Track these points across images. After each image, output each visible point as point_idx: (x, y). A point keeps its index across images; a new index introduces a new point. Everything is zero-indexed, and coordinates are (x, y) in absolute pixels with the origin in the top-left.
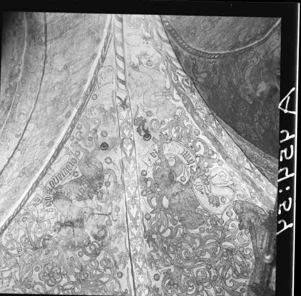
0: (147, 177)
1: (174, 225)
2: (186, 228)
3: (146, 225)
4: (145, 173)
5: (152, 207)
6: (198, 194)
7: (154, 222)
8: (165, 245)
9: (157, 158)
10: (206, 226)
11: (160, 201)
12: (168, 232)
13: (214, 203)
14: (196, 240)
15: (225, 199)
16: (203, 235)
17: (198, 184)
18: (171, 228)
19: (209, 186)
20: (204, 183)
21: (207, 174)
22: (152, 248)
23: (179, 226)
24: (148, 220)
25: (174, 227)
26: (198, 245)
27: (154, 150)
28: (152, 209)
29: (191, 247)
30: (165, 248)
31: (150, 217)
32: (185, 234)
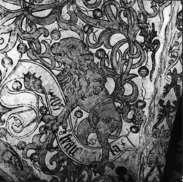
0: (132, 124)
1: (102, 50)
2: (82, 42)
3: (150, 60)
4: (134, 130)
5: (133, 84)
6: (57, 92)
7: (135, 61)
8: (125, 20)
9: (112, 145)
10: (49, 42)
11: (119, 87)
12: (116, 38)
13: (32, 80)
14: (67, 17)
15: (15, 87)
16: (53, 26)
17: (57, 107)
18: (108, 45)
19: (41, 105)
20: (47, 110)
21: (42, 123)
22: (151, 21)
23: (95, 46)
24: (145, 68)
25: (102, 47)
26: (65, 10)
27: (114, 155)
28: (134, 80)
29: (78, 7)
30: (126, 16)
31: (139, 71)
32: (86, 33)
